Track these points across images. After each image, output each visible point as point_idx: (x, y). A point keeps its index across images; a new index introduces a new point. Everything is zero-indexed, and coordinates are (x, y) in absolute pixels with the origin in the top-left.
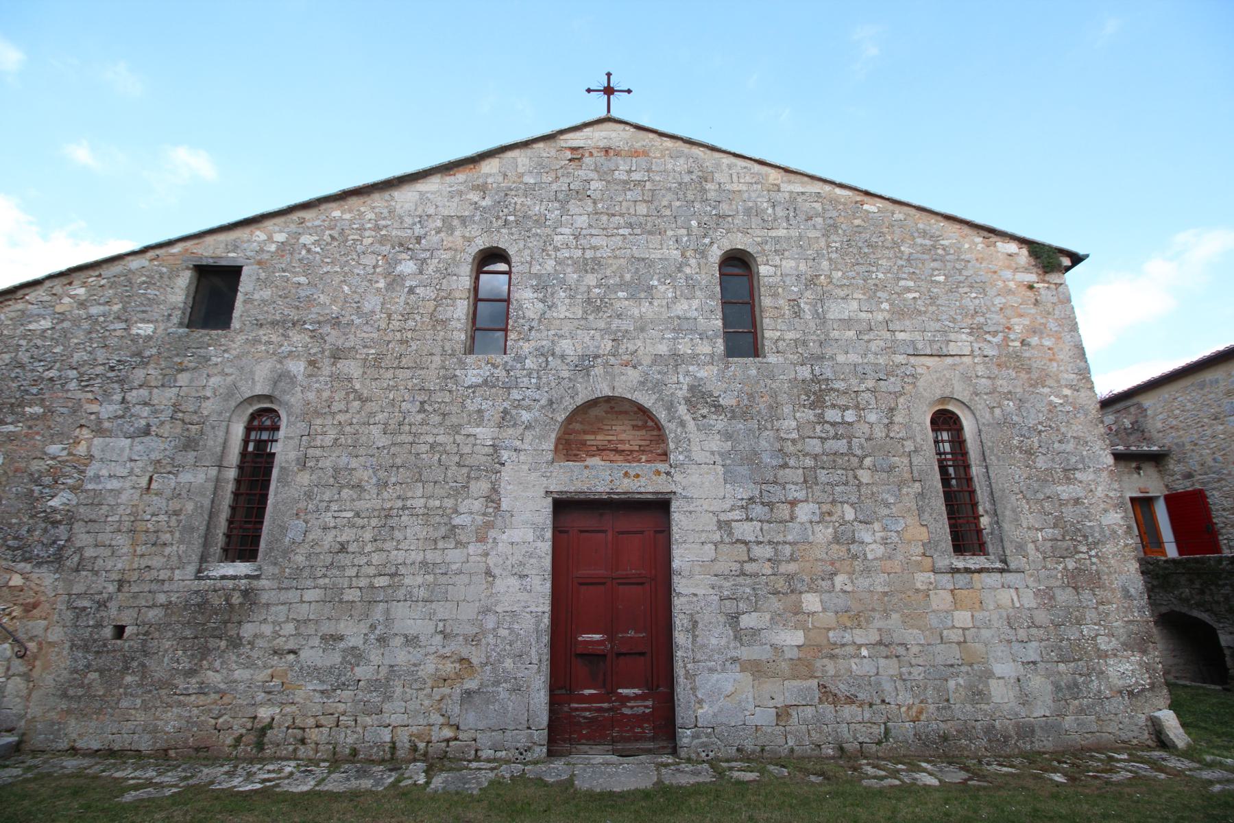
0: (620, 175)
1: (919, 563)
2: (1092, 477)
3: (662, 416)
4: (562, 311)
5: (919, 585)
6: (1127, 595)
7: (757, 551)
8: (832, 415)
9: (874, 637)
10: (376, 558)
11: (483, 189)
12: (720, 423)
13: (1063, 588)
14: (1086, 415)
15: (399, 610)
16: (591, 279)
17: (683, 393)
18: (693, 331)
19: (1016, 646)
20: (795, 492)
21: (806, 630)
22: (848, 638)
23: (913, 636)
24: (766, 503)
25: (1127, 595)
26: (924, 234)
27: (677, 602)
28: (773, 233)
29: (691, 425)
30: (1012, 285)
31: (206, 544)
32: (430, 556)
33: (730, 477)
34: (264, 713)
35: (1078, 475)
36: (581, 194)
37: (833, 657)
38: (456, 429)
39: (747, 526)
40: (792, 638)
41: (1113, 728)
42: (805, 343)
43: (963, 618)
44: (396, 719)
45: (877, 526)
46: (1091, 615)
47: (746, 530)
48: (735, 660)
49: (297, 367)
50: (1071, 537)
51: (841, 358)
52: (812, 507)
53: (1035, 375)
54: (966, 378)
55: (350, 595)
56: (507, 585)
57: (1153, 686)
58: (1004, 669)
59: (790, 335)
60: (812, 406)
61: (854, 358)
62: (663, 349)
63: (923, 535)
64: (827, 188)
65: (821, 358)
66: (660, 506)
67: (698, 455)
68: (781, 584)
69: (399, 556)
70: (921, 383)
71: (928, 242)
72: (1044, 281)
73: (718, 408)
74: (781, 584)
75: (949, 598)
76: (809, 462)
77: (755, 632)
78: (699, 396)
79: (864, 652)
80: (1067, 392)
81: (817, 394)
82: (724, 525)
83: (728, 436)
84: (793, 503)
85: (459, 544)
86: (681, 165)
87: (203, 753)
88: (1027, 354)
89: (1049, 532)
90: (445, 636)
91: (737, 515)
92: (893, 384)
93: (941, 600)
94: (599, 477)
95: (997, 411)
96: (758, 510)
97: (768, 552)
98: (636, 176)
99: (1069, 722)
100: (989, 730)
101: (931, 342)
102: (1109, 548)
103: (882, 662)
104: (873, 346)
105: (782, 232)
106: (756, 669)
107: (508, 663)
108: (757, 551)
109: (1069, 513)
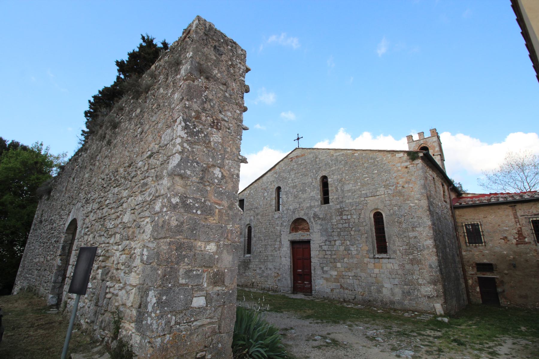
0: (300, 162)
1: (365, 256)
2: (422, 229)
3: (308, 221)
4: (290, 199)
5: (365, 262)
6: (431, 267)
7: (327, 253)
8: (345, 217)
9: (353, 274)
10: (265, 254)
11: (276, 173)
12: (319, 222)
13: (408, 264)
14: (422, 208)
15: (269, 263)
16: (295, 190)
17: (312, 215)
18: (314, 199)
19: (391, 279)
20: (336, 238)
21: (338, 272)
22: (347, 274)
23: (363, 275)
24: (329, 241)
25: (431, 267)
26: (371, 158)
27: (312, 264)
28: (332, 169)
29: (314, 223)
30: (400, 168)
31: (244, 251)
32: (272, 253)
33: (322, 235)
34: (253, 280)
35: (417, 229)
36: (292, 170)
37: (343, 278)
38: (274, 228)
39: (325, 246)
40: (334, 273)
41: (421, 306)
42: (338, 198)
43: (376, 271)
44: (269, 283)
45: (355, 246)
46: (417, 272)
47: (325, 248)
48: (323, 277)
49: (252, 218)
50: (412, 248)
51: (347, 201)
52: (340, 241)
53: (405, 197)
54: (382, 202)
55: (262, 260)
56: (283, 259)
57: (437, 296)
58: (387, 285)
59: (335, 197)
60: (340, 215)
61: (350, 201)
62: (308, 205)
63: (367, 248)
64: (345, 151)
65: (342, 202)
66: (308, 242)
67: (315, 230)
68: (332, 261)
69: (268, 253)
70: (368, 205)
71: (372, 161)
72: (412, 164)
73: (319, 218)
74: (332, 261)
75: (373, 265)
76: (339, 230)
77: (327, 271)
78: (315, 216)
79: (351, 278)
80: (416, 201)
81: (341, 212)
82: (321, 246)
83: (321, 225)
84: (335, 241)
85: (276, 251)
86: (311, 155)
87: (246, 286)
88: (403, 191)
89: (404, 247)
90: (275, 268)
91: (323, 244)
92: (360, 207)
93: (371, 266)
94: (299, 236)
95: (391, 211)
96: (328, 243)
97: (329, 253)
98: (303, 162)
99: (406, 302)
100: (382, 301)
101: (372, 192)
102: (426, 252)
103: (355, 281)
104: (356, 197)
105: (334, 168)
106: (327, 280)
107: (284, 275)
108: (327, 253)
109: (412, 241)
